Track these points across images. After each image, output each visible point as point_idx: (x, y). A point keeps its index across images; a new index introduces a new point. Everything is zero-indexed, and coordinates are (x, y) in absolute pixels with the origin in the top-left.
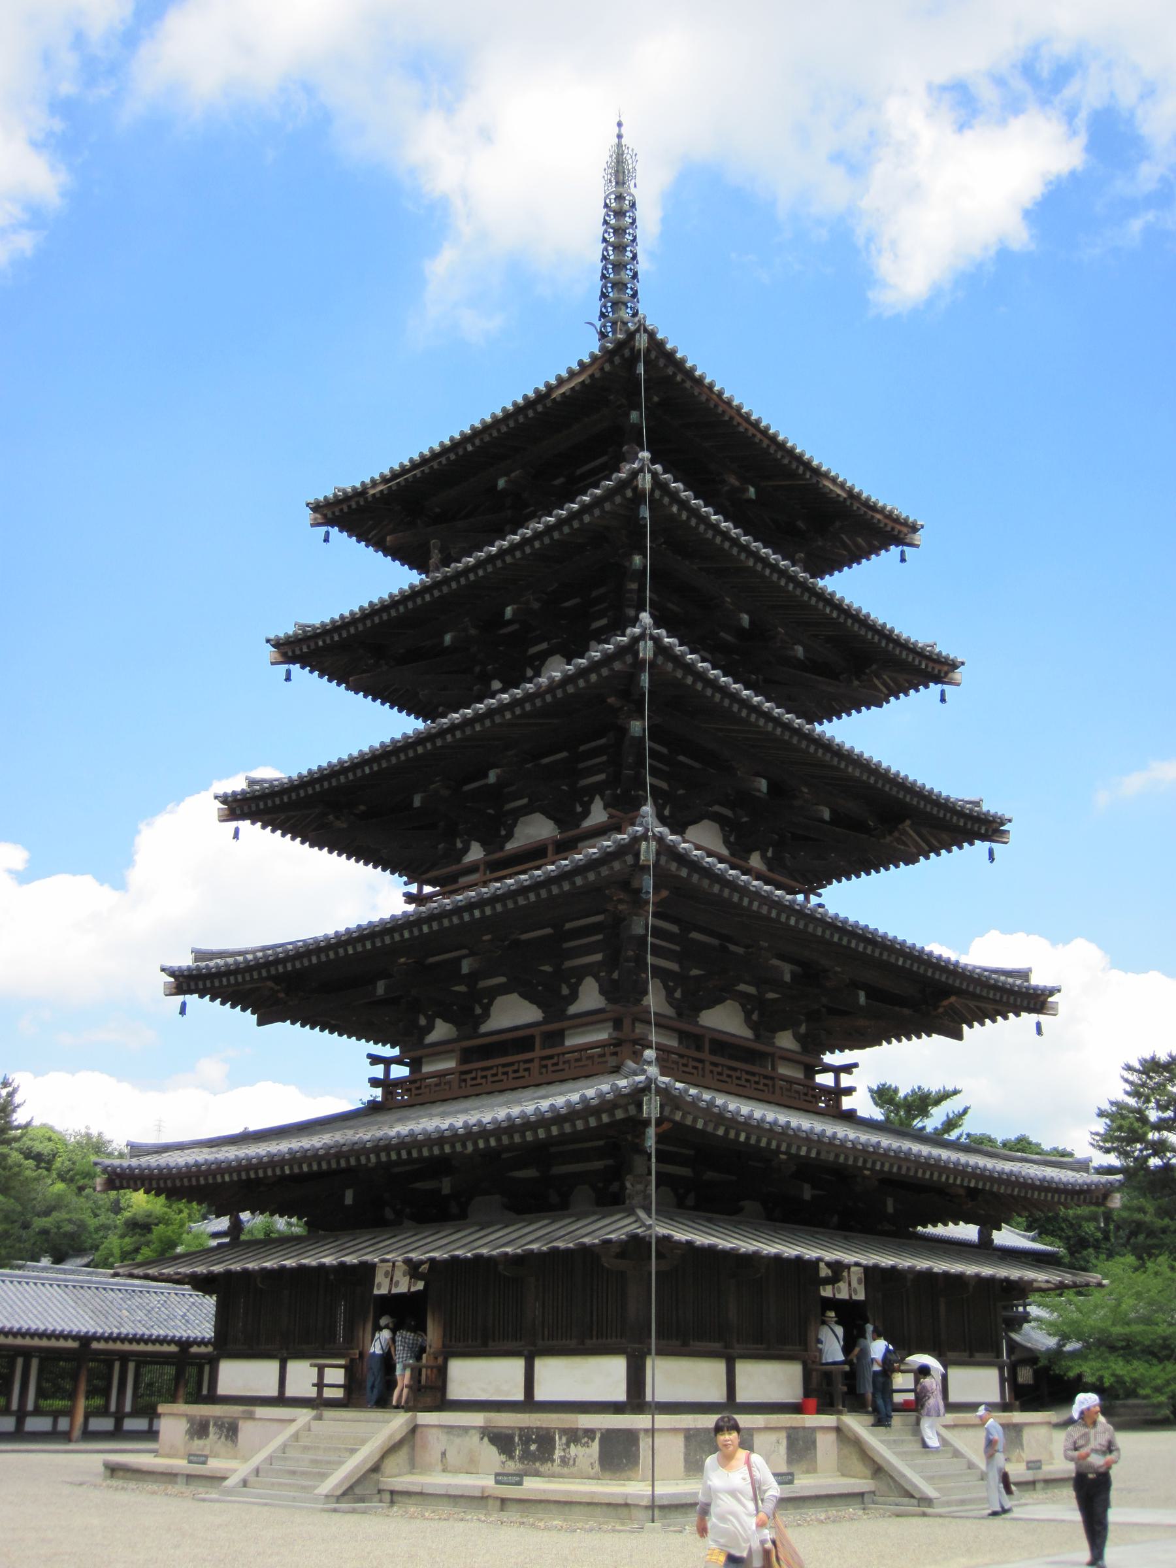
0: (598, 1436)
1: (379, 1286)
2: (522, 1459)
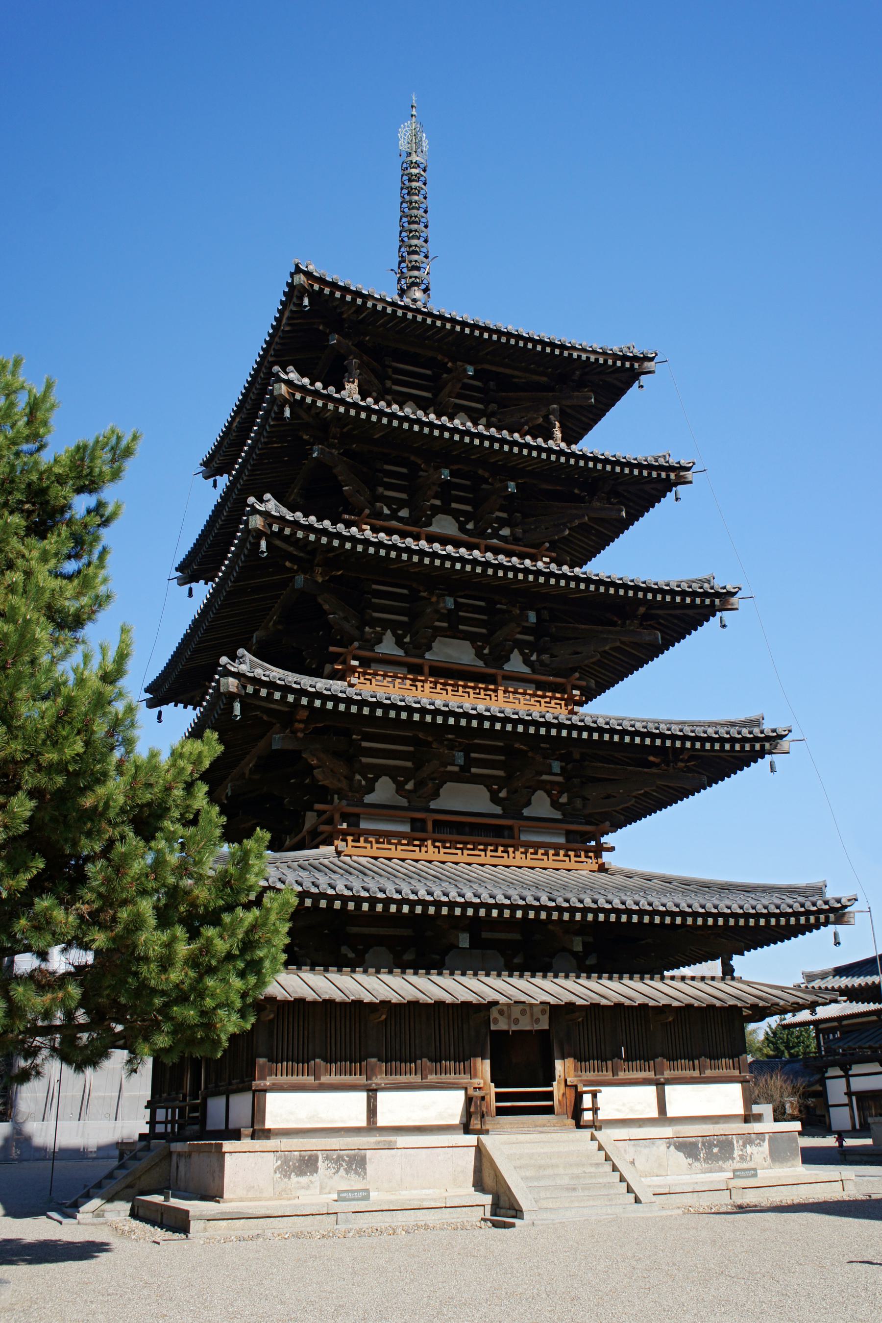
0: (767, 1136)
1: (496, 1021)
2: (706, 1160)
